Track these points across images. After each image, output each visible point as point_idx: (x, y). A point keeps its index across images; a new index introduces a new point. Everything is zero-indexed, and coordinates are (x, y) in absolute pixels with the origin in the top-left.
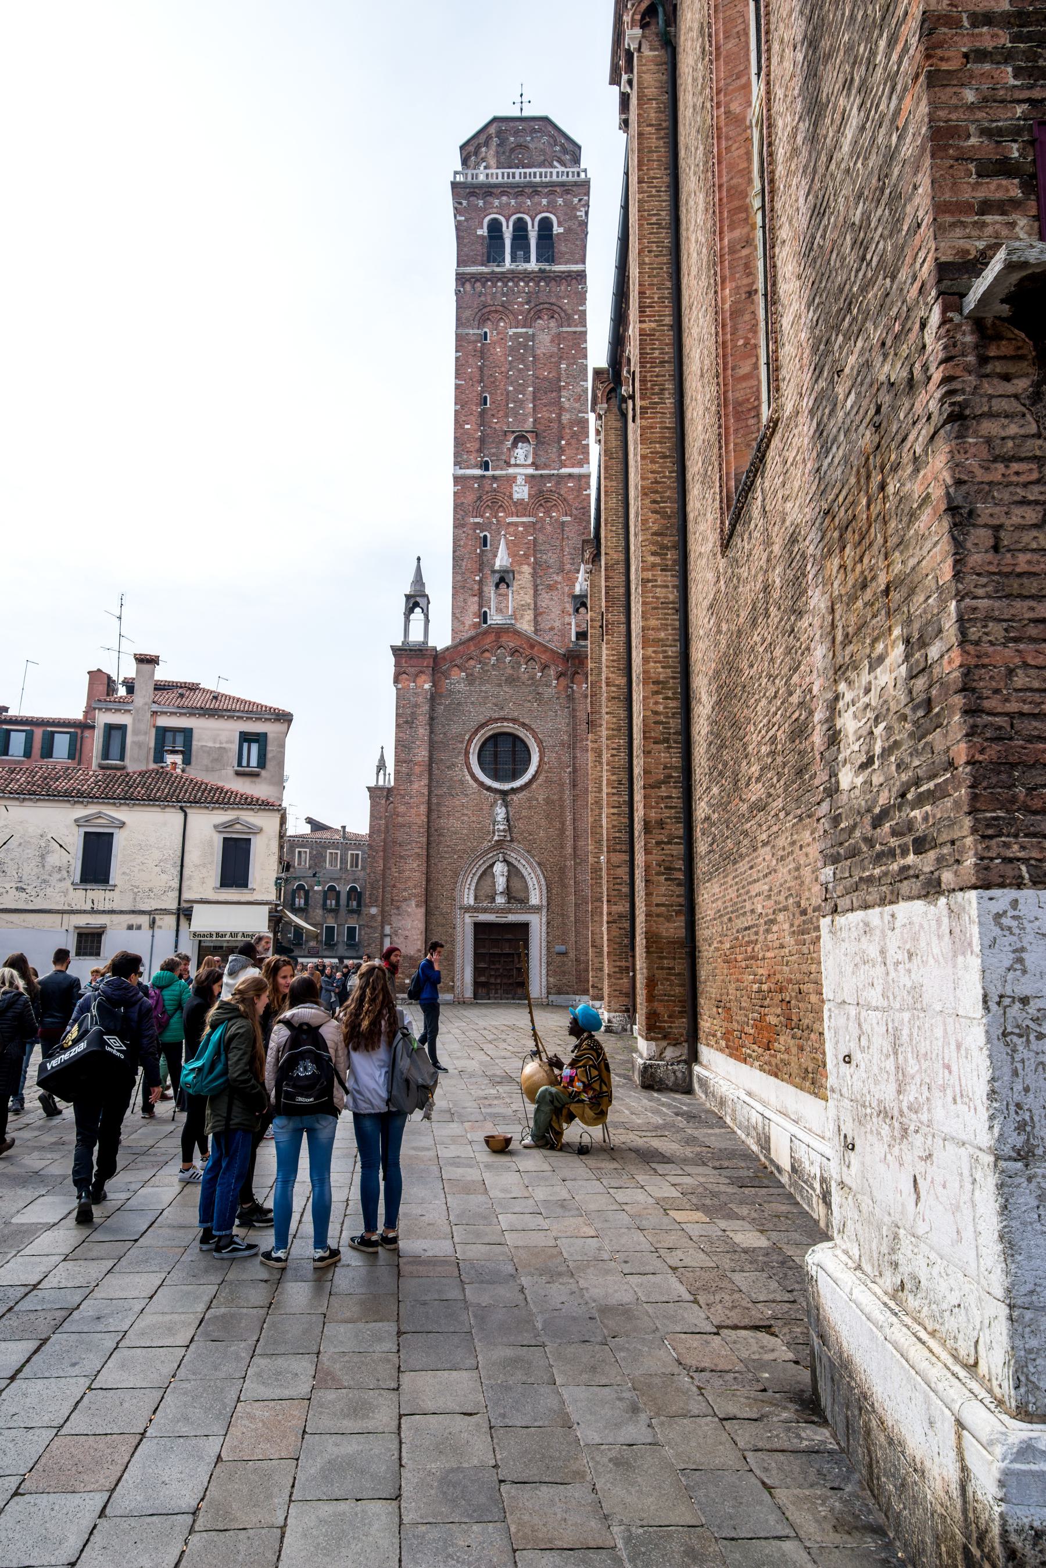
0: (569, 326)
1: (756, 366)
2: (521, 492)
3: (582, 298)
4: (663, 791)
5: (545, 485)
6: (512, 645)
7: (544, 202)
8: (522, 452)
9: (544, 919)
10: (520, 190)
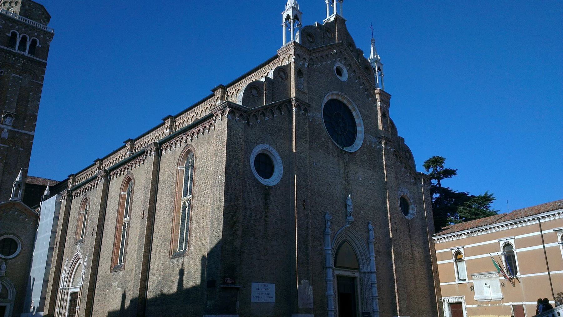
0: (37, 81)
1: (178, 235)
2: (5, 135)
3: (44, 72)
5: (15, 135)
7: (36, 34)
8: (8, 120)
9: (13, 305)
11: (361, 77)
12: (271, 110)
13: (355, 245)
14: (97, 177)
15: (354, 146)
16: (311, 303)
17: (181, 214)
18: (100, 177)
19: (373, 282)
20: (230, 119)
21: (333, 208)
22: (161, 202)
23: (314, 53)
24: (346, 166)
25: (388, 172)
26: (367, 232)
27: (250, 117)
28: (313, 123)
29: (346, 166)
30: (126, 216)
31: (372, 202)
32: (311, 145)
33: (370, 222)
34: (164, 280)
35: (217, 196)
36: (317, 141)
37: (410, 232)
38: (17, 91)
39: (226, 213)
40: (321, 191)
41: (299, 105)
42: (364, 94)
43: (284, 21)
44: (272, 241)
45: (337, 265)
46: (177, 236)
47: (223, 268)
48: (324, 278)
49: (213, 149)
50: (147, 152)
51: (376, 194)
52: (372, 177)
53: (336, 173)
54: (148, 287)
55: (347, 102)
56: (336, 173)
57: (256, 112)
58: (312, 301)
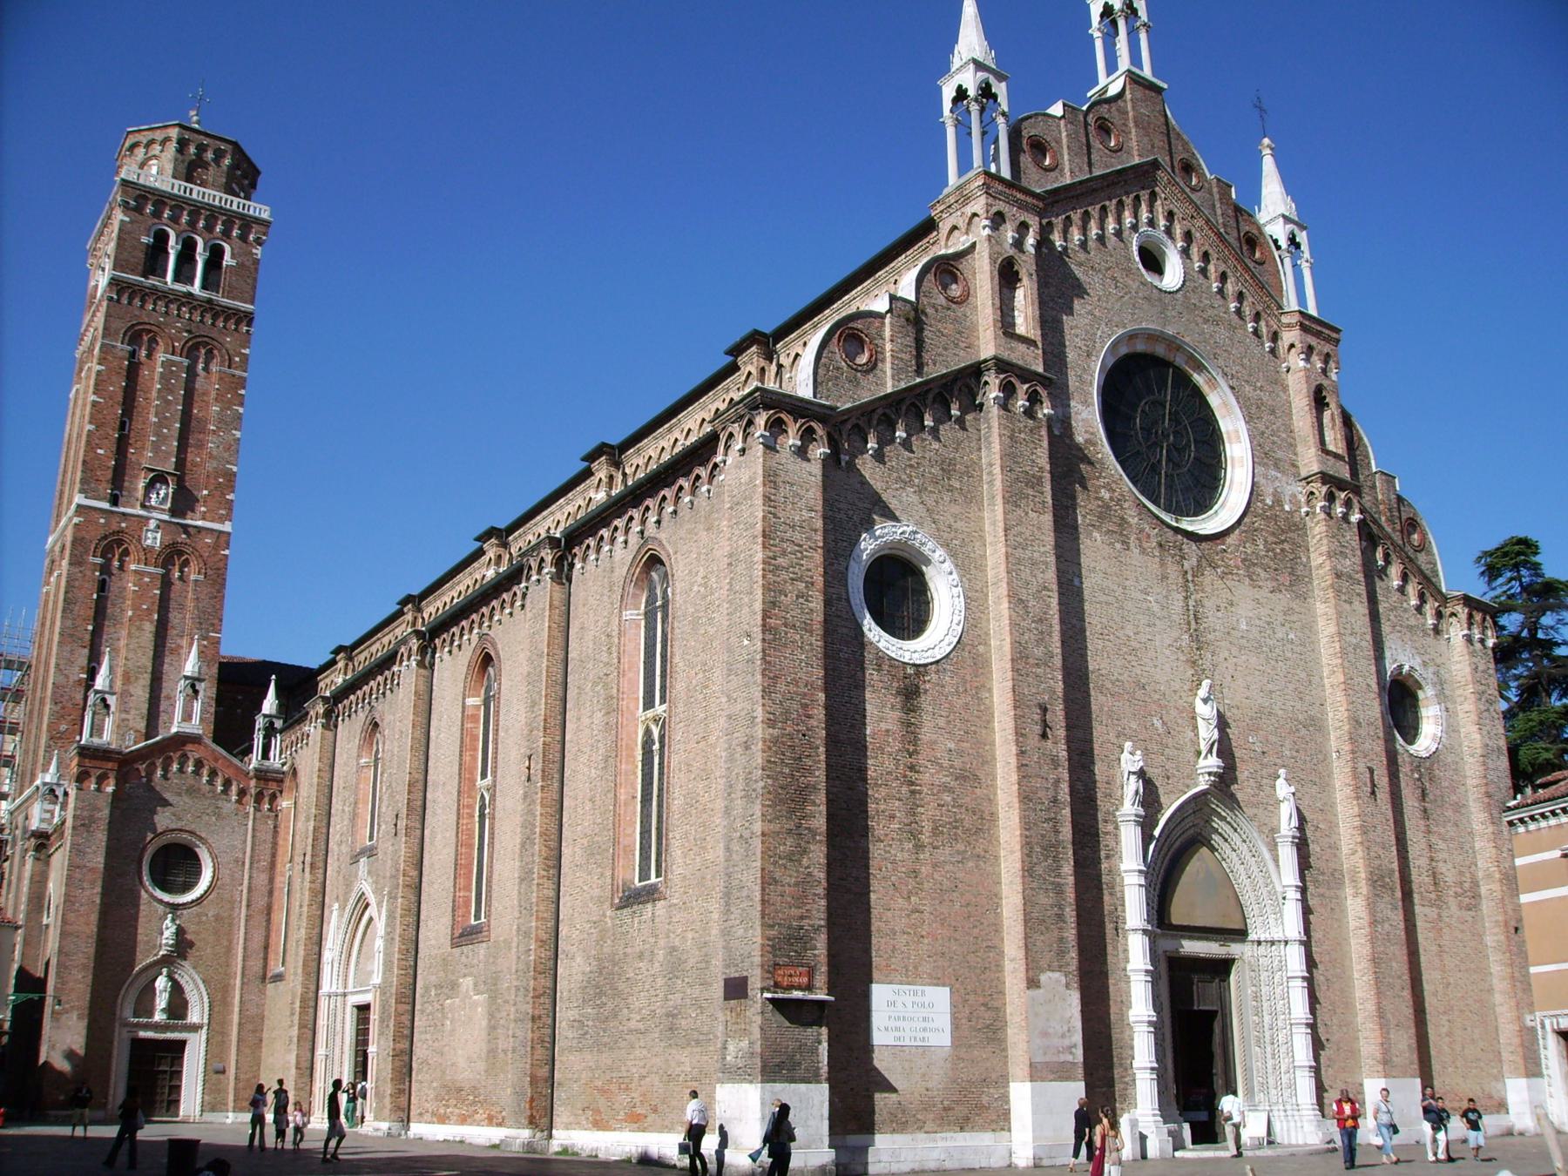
2: (153, 539)
4: (542, 1000)
6: (197, 756)
9: (204, 1037)
10: (196, 209)
12: (913, 404)
13: (1228, 851)
14: (397, 652)
16: (1075, 1046)
17: (640, 764)
18: (406, 655)
22: (578, 730)
23: (1057, 202)
24: (1190, 585)
25: (1343, 597)
27: (841, 434)
29: (1190, 585)
30: (484, 776)
31: (1288, 703)
33: (1282, 772)
34: (601, 973)
35: (739, 707)
37: (1424, 800)
38: (177, 404)
40: (1103, 672)
42: (1246, 330)
43: (947, 105)
46: (629, 835)
47: (769, 939)
48: (1122, 965)
49: (722, 550)
50: (530, 568)
51: (1303, 675)
53: (1156, 608)
54: (558, 994)
56: (1156, 608)
57: (863, 415)
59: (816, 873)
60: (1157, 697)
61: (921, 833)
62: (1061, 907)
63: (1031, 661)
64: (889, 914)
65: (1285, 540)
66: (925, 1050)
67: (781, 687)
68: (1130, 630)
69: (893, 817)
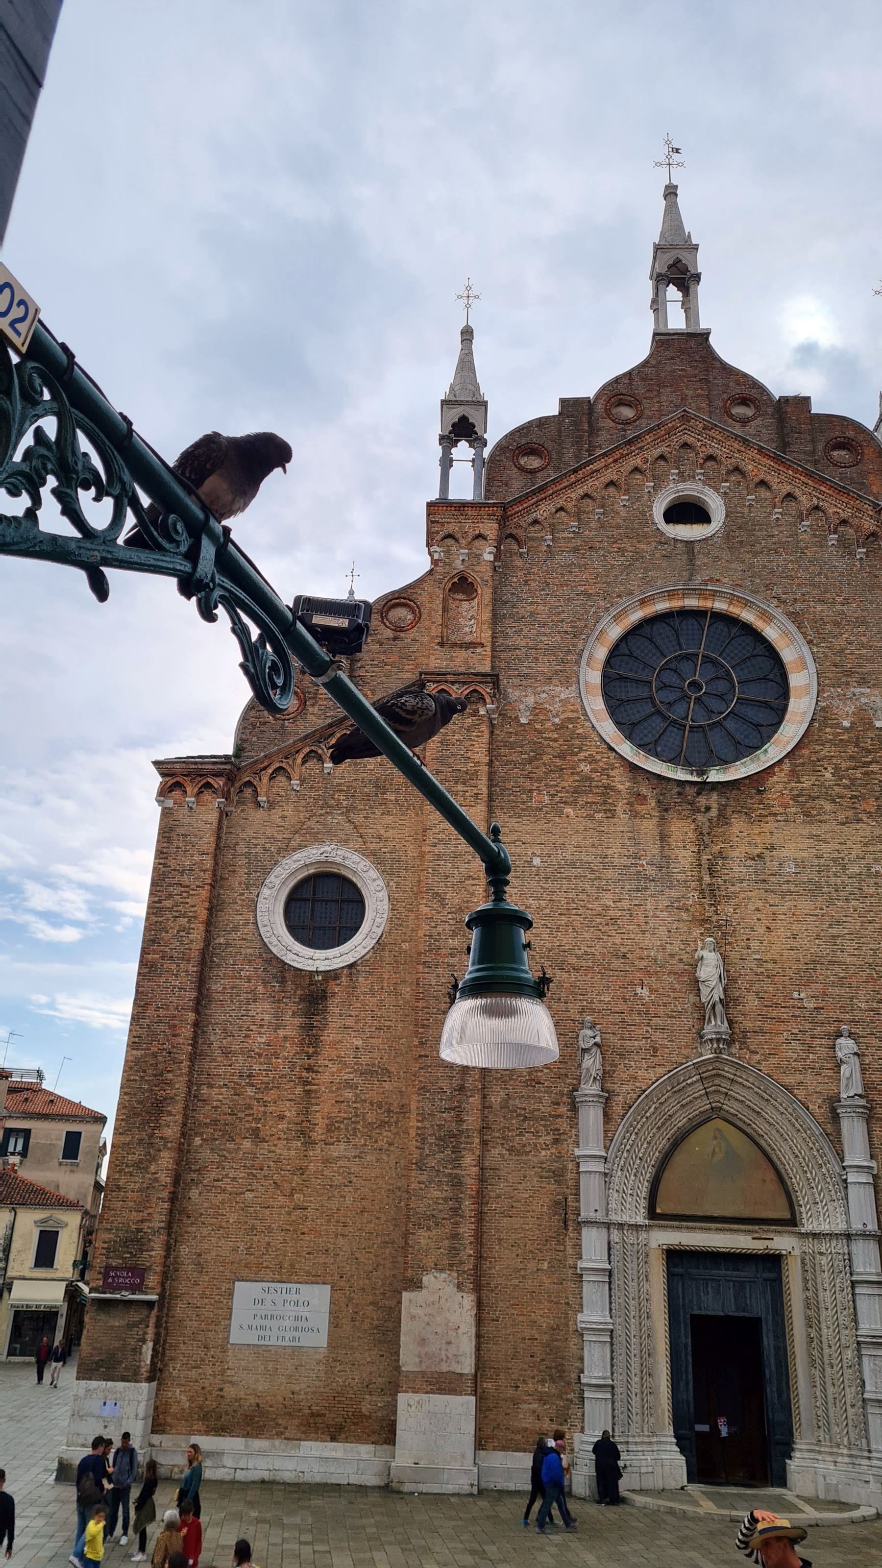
11: (797, 493)
15: (766, 750)
19: (858, 1274)
20: (170, 809)
21: (625, 1000)
26: (830, 1073)
28: (538, 726)
32: (523, 803)
36: (552, 783)
39: (132, 1078)
41: (443, 690)
44: (325, 1144)
45: (658, 1211)
48: (570, 1262)
52: (871, 848)
53: (651, 871)
55: (730, 603)
56: (651, 871)
57: (286, 758)
58: (467, 1345)
59: (163, 1178)
60: (643, 964)
61: (311, 1131)
62: (457, 1200)
63: (444, 951)
64: (267, 1211)
65: (871, 763)
66: (296, 1351)
67: (151, 1012)
68: (608, 899)
69: (282, 1117)
